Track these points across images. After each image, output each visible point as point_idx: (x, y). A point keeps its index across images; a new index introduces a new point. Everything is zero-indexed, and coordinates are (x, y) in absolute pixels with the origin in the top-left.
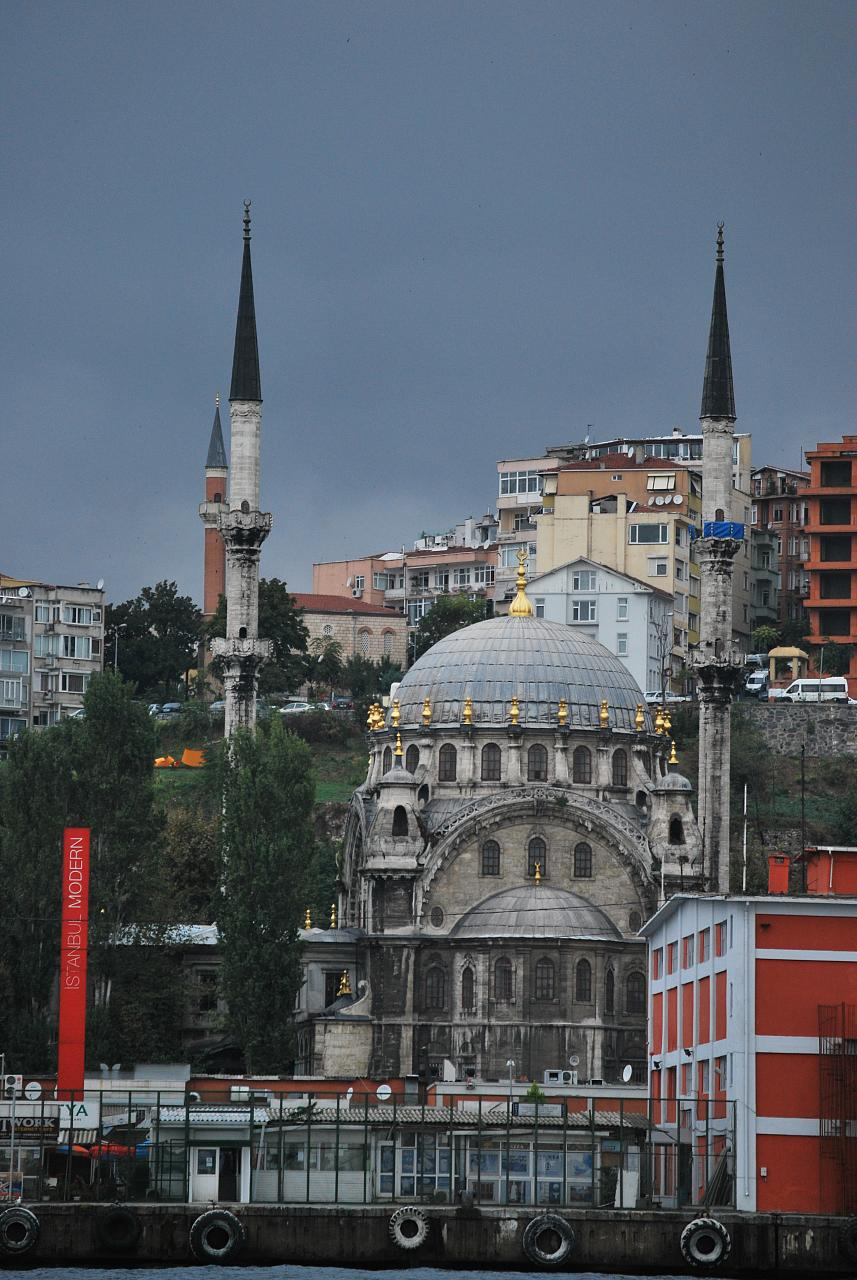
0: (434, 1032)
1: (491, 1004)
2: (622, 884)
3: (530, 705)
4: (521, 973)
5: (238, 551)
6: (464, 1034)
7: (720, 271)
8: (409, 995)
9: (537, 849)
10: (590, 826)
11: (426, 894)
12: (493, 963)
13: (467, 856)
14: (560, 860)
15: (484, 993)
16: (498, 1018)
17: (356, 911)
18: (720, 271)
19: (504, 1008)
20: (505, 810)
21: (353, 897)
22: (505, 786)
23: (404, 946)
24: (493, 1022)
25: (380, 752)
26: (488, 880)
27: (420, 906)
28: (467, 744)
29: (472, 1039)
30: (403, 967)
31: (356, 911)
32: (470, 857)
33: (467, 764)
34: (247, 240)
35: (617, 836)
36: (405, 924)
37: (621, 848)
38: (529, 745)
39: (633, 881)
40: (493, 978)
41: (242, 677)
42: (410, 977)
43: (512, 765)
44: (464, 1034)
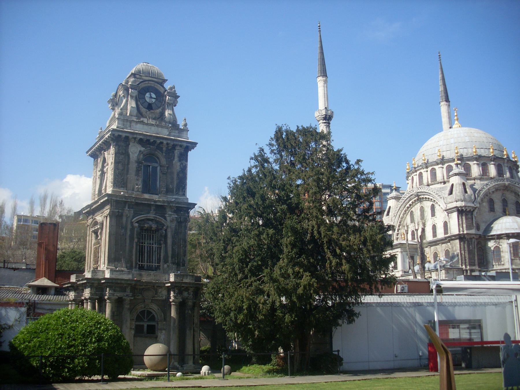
5: (325, 123)
8: (476, 258)
9: (505, 202)
13: (484, 204)
14: (511, 207)
16: (515, 265)
17: (403, 236)
21: (398, 231)
22: (491, 178)
28: (475, 162)
31: (403, 236)
33: (475, 170)
38: (497, 164)
40: (512, 249)
42: (476, 250)
43: (492, 171)
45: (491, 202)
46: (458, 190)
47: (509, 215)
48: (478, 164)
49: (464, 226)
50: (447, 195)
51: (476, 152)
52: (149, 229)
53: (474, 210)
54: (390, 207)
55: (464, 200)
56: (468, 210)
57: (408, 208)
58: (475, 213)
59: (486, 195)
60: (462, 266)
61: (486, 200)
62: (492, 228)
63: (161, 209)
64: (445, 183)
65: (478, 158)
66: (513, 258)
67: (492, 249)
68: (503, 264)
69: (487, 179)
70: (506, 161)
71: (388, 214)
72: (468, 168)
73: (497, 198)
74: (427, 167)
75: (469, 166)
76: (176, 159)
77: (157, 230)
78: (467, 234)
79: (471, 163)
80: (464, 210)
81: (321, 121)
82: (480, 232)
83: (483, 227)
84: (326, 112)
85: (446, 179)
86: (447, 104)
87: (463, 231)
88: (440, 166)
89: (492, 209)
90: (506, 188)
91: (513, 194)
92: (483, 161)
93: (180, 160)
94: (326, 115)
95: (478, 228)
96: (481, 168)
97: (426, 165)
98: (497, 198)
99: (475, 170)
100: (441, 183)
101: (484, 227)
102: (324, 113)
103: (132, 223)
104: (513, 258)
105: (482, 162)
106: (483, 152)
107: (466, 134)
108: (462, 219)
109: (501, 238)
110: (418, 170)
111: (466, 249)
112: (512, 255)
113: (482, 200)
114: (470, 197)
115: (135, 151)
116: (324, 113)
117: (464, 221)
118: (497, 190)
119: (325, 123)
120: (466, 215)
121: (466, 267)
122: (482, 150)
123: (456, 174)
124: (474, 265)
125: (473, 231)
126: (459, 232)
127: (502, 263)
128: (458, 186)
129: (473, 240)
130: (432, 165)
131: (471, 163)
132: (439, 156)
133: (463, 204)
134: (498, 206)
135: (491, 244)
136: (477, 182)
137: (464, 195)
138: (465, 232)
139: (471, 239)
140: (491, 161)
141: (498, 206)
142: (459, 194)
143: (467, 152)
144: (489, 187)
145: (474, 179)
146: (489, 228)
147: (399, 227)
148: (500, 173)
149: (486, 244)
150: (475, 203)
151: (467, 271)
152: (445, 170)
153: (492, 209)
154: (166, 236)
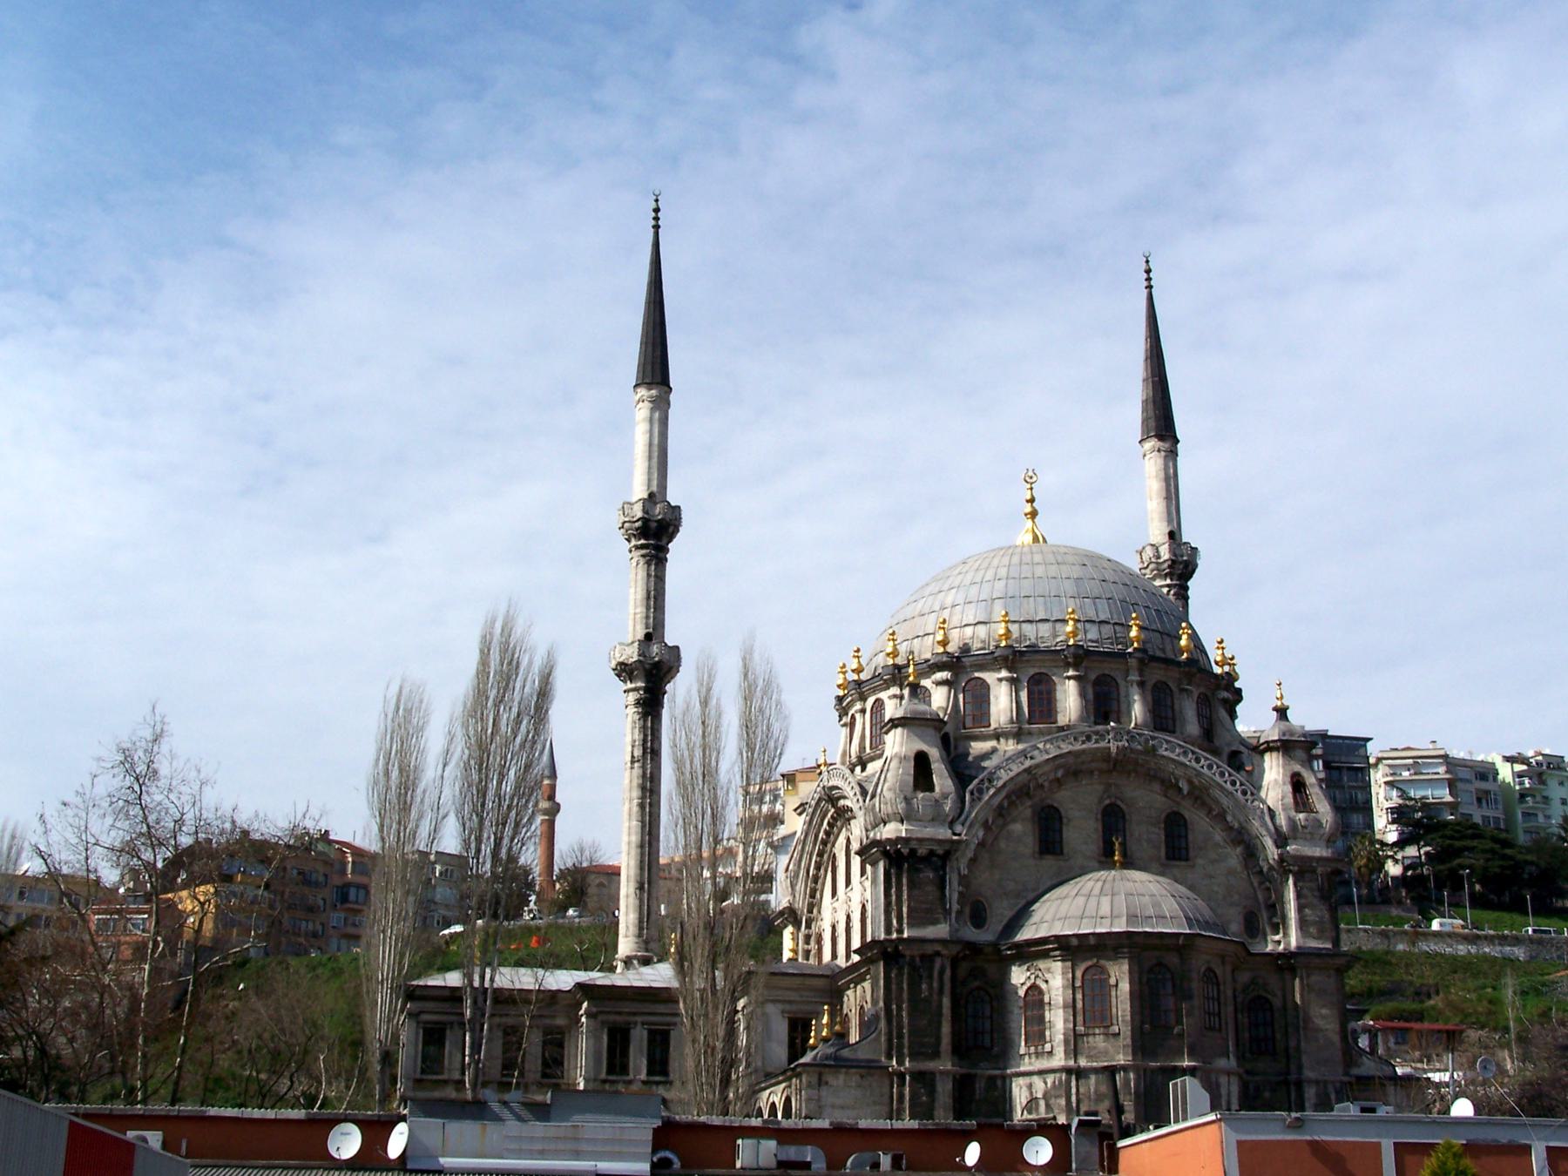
0: (980, 1086)
1: (1076, 1036)
2: (1231, 872)
3: (1088, 625)
4: (1125, 986)
5: (642, 547)
6: (1030, 1086)
8: (946, 1029)
9: (1113, 820)
10: (1184, 785)
11: (963, 880)
12: (1079, 974)
13: (1017, 827)
14: (1146, 833)
15: (1066, 1021)
16: (1090, 1058)
17: (813, 945)
19: (1099, 1042)
20: (1071, 760)
21: (808, 926)
22: (1062, 729)
23: (938, 954)
24: (1083, 1062)
25: (863, 711)
26: (1049, 861)
27: (955, 896)
28: (1004, 674)
29: (1045, 1097)
30: (935, 985)
31: (813, 945)
32: (1021, 829)
33: (1002, 702)
35: (1225, 801)
36: (935, 922)
37: (1229, 818)
38: (1093, 676)
39: (1246, 867)
40: (1079, 996)
41: (646, 690)
42: (946, 1002)
43: (1069, 699)
44: (1030, 1086)
47: (1128, 864)
48: (1013, 682)
53: (946, 856)
56: (922, 851)
57: (824, 843)
59: (1020, 790)
60: (889, 1057)
65: (1012, 658)
66: (1081, 1029)
67: (1022, 993)
70: (1133, 662)
72: (980, 697)
74: (863, 699)
75: (985, 686)
78: (910, 940)
79: (989, 677)
80: (905, 851)
81: (634, 542)
82: (984, 936)
84: (645, 511)
86: (1165, 445)
87: (900, 931)
88: (895, 690)
90: (1118, 765)
91: (1156, 787)
94: (645, 520)
101: (1009, 914)
104: (1081, 1029)
105: (1032, 671)
106: (1041, 634)
109: (1045, 955)
111: (905, 996)
112: (1080, 1018)
114: (937, 803)
116: (639, 514)
119: (642, 547)
120: (914, 870)
121: (900, 1063)
122: (1045, 630)
125: (941, 930)
126: (888, 931)
127: (1048, 1047)
129: (938, 961)
130: (875, 690)
131: (989, 677)
134: (1081, 832)
135: (1019, 976)
136: (1010, 746)
137: (907, 800)
139: (928, 959)
140: (1067, 666)
141: (1081, 832)
145: (997, 736)
146: (1021, 916)
147: (810, 911)
148: (1102, 705)
149: (1006, 975)
150: (958, 828)
151: (902, 1076)
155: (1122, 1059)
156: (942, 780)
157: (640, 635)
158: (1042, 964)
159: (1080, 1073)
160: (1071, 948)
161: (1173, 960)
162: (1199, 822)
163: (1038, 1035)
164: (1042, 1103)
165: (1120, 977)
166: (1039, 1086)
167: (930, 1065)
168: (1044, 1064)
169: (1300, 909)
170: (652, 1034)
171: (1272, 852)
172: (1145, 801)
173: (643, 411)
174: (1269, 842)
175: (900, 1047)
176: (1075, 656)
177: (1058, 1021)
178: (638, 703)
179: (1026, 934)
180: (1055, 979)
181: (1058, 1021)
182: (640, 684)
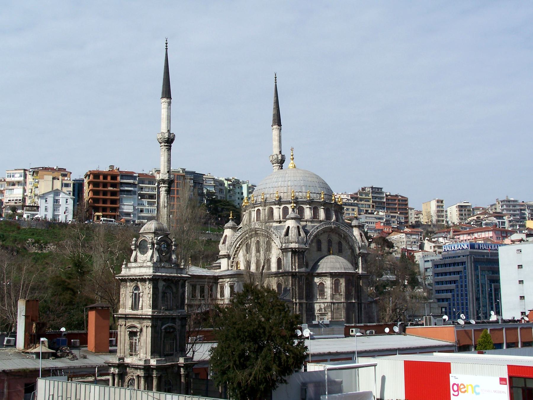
4: (344, 284)
5: (166, 146)
6: (320, 306)
7: (276, 85)
9: (330, 242)
13: (313, 244)
14: (335, 246)
16: (336, 300)
18: (276, 85)
19: (338, 296)
21: (233, 259)
22: (321, 221)
24: (334, 301)
28: (308, 206)
29: (324, 308)
33: (308, 213)
34: (167, 49)
41: (168, 187)
43: (322, 215)
44: (320, 306)
45: (319, 243)
46: (293, 233)
47: (333, 254)
48: (310, 208)
49: (297, 264)
50: (282, 236)
51: (309, 197)
52: (169, 332)
54: (226, 236)
55: (298, 242)
58: (306, 253)
59: (316, 236)
60: (293, 299)
61: (315, 241)
62: (319, 266)
63: (173, 319)
64: (280, 222)
67: (318, 284)
68: (326, 298)
69: (317, 222)
70: (333, 205)
71: (224, 243)
72: (301, 211)
73: (324, 239)
74: (265, 206)
75: (303, 208)
76: (180, 287)
77: (173, 332)
78: (298, 272)
79: (304, 206)
81: (163, 144)
82: (308, 270)
83: (311, 265)
85: (281, 219)
86: (279, 128)
88: (277, 206)
89: (319, 249)
90: (331, 230)
91: (337, 235)
92: (314, 205)
93: (182, 288)
95: (307, 266)
96: (312, 211)
97: (265, 203)
98: (324, 239)
99: (308, 213)
100: (277, 222)
101: (312, 265)
102: (166, 136)
103: (161, 329)
105: (314, 206)
107: (301, 178)
108: (295, 260)
109: (326, 276)
110: (257, 207)
113: (312, 241)
114: (303, 239)
115: (161, 284)
116: (167, 137)
117: (297, 261)
118: (324, 232)
119: (166, 146)
120: (298, 255)
122: (315, 195)
123: (292, 219)
124: (303, 299)
125: (303, 270)
127: (325, 297)
128: (293, 229)
131: (304, 206)
132: (278, 197)
133: (297, 246)
134: (324, 246)
135: (317, 280)
136: (309, 224)
138: (297, 270)
139: (301, 276)
140: (322, 205)
141: (324, 246)
142: (294, 237)
143: (302, 195)
144: (318, 230)
145: (306, 221)
146: (316, 266)
147: (234, 255)
148: (328, 217)
151: (296, 303)
152: (281, 210)
153: (319, 249)
154: (176, 336)
155: (343, 301)
156: (303, 234)
157: (166, 170)
158: (324, 278)
159: (334, 303)
160: (332, 275)
161: (351, 278)
162: (344, 243)
163: (322, 293)
164: (323, 310)
165: (343, 282)
166: (323, 306)
167: (302, 301)
168: (324, 301)
169: (362, 264)
170: (201, 287)
171: (358, 252)
172: (335, 238)
173: (164, 106)
174: (357, 249)
175: (296, 297)
176: (324, 204)
177: (328, 291)
178: (166, 191)
179: (319, 271)
180: (328, 282)
181: (328, 291)
182: (167, 185)
